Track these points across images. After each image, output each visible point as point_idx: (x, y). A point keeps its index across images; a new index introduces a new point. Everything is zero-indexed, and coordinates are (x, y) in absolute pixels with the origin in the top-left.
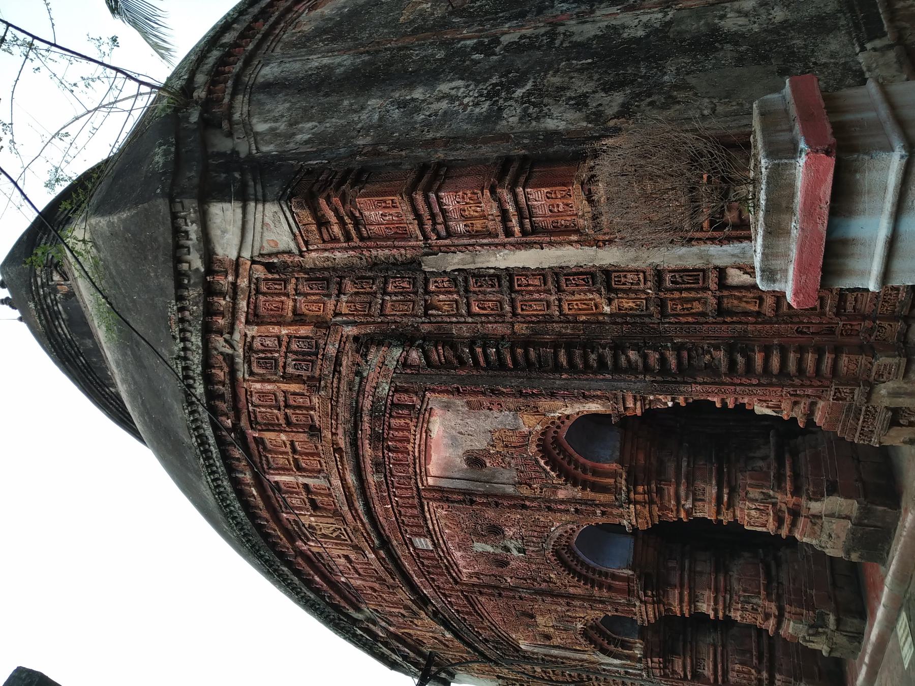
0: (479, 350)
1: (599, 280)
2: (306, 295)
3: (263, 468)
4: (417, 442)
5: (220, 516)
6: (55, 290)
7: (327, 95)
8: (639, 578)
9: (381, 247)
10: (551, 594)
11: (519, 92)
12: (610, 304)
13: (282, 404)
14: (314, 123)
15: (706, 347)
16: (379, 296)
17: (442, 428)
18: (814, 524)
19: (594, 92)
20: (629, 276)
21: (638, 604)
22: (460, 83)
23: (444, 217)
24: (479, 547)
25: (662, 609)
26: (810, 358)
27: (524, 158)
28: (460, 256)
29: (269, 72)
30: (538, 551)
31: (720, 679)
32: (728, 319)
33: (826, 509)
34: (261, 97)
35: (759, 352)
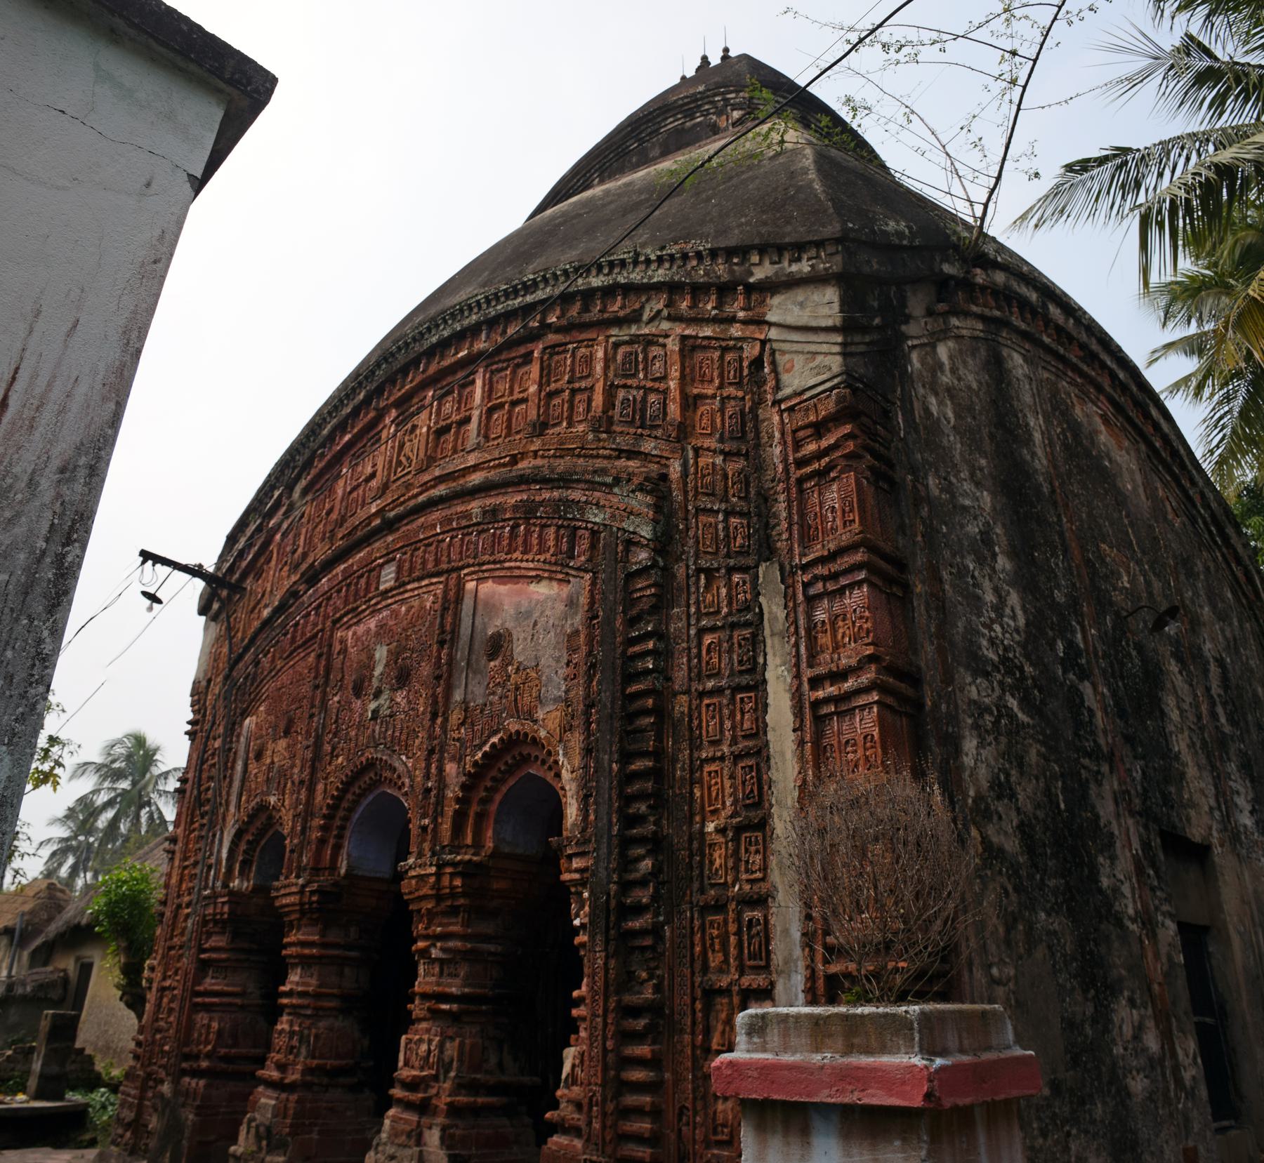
0: (651, 645)
1: (752, 814)
2: (722, 410)
4: (524, 565)
5: (432, 311)
6: (720, 113)
7: (992, 437)
8: (336, 884)
9: (789, 507)
10: (316, 758)
12: (719, 831)
13: (577, 385)
14: (952, 420)
15: (658, 972)
16: (723, 506)
17: (542, 598)
18: (409, 1135)
19: (1018, 810)
20: (758, 858)
21: (301, 881)
23: (834, 591)
24: (381, 653)
25: (293, 917)
26: (644, 1126)
27: (920, 705)
28: (781, 614)
29: (1017, 362)
31: (199, 1000)
32: (698, 1005)
33: (430, 1153)
34: (983, 352)
35: (653, 1051)
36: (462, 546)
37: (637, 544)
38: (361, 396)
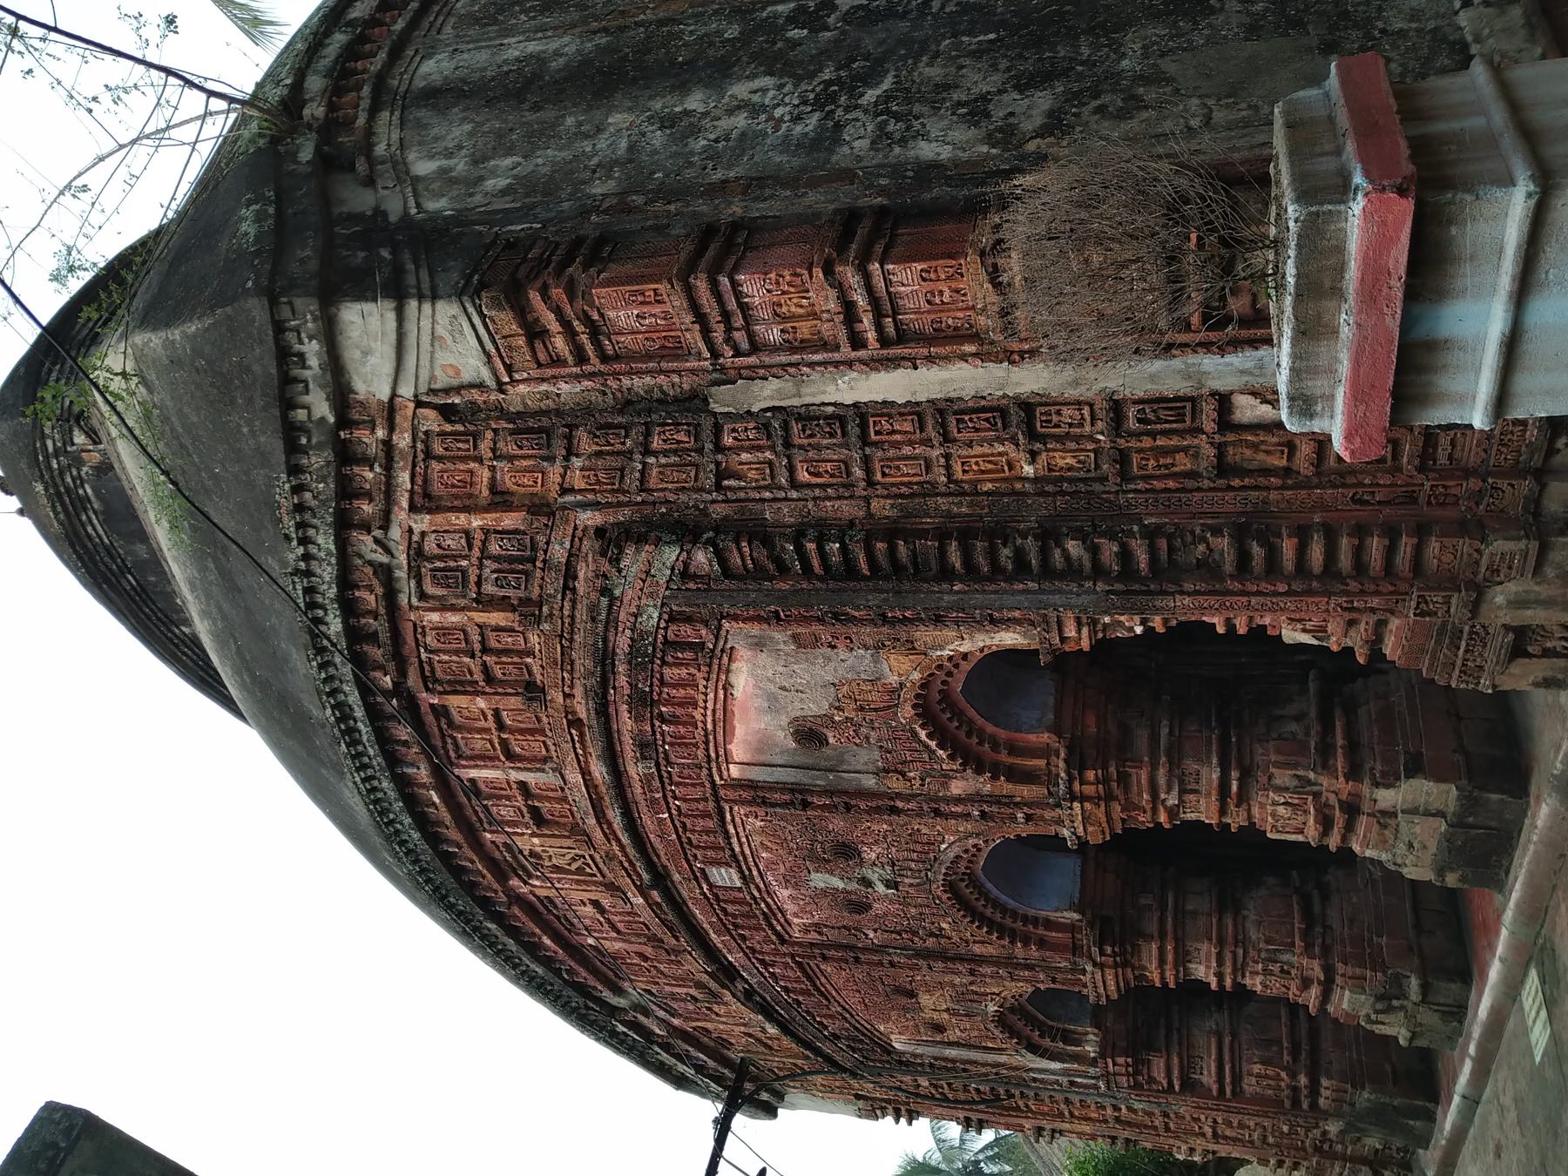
0: (811, 546)
1: (1014, 420)
2: (511, 458)
3: (449, 757)
4: (710, 705)
5: (377, 840)
6: (78, 461)
7: (536, 107)
8: (1091, 925)
9: (639, 373)
11: (871, 95)
12: (1033, 461)
13: (477, 647)
14: (516, 159)
16: (637, 457)
17: (751, 681)
18: (1384, 826)
19: (1000, 92)
20: (1066, 411)
21: (1089, 968)
22: (767, 81)
23: (745, 318)
24: (819, 880)
25: (1130, 976)
26: (1376, 545)
27: (882, 212)
28: (774, 384)
29: (433, 69)
30: (918, 885)
31: (1228, 1090)
32: (1236, 482)
33: (1404, 801)
34: (422, 113)
35: (1289, 536)
36: (685, 785)
37: (686, 565)
38: (492, 926)
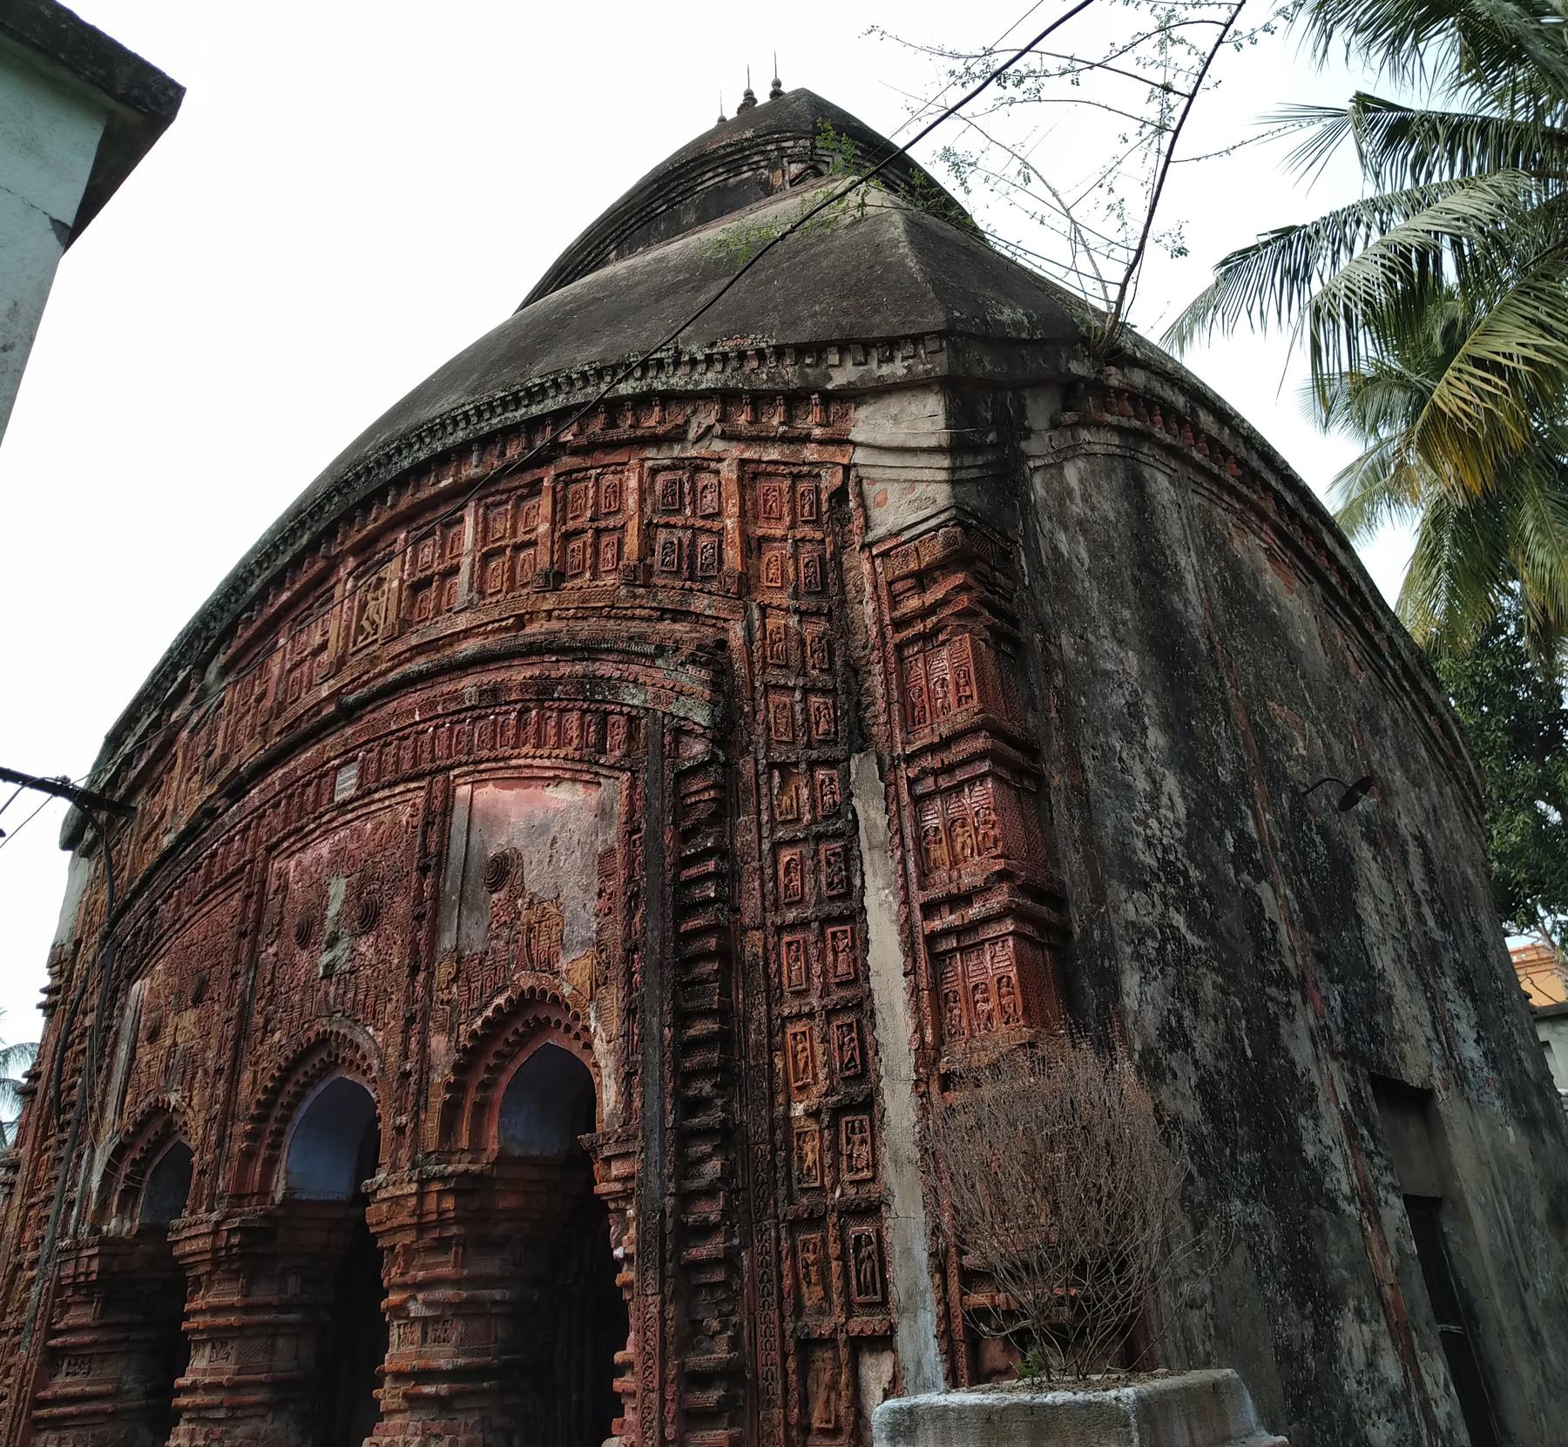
0: (711, 866)
1: (854, 1090)
2: (795, 556)
3: (487, 496)
4: (537, 762)
5: (403, 426)
7: (1136, 581)
8: (267, 1216)
9: (887, 682)
10: (242, 1034)
11: (1179, 920)
13: (602, 524)
14: (1087, 561)
15: (734, 1319)
16: (801, 681)
17: (562, 806)
19: (1195, 1062)
20: (866, 1149)
22: (1182, 811)
23: (948, 789)
24: (338, 889)
25: (201, 1270)
27: (1066, 934)
28: (881, 821)
30: (327, 1002)
32: (792, 1364)
35: (730, 1437)
36: (450, 738)
37: (690, 733)
38: (305, 540)
